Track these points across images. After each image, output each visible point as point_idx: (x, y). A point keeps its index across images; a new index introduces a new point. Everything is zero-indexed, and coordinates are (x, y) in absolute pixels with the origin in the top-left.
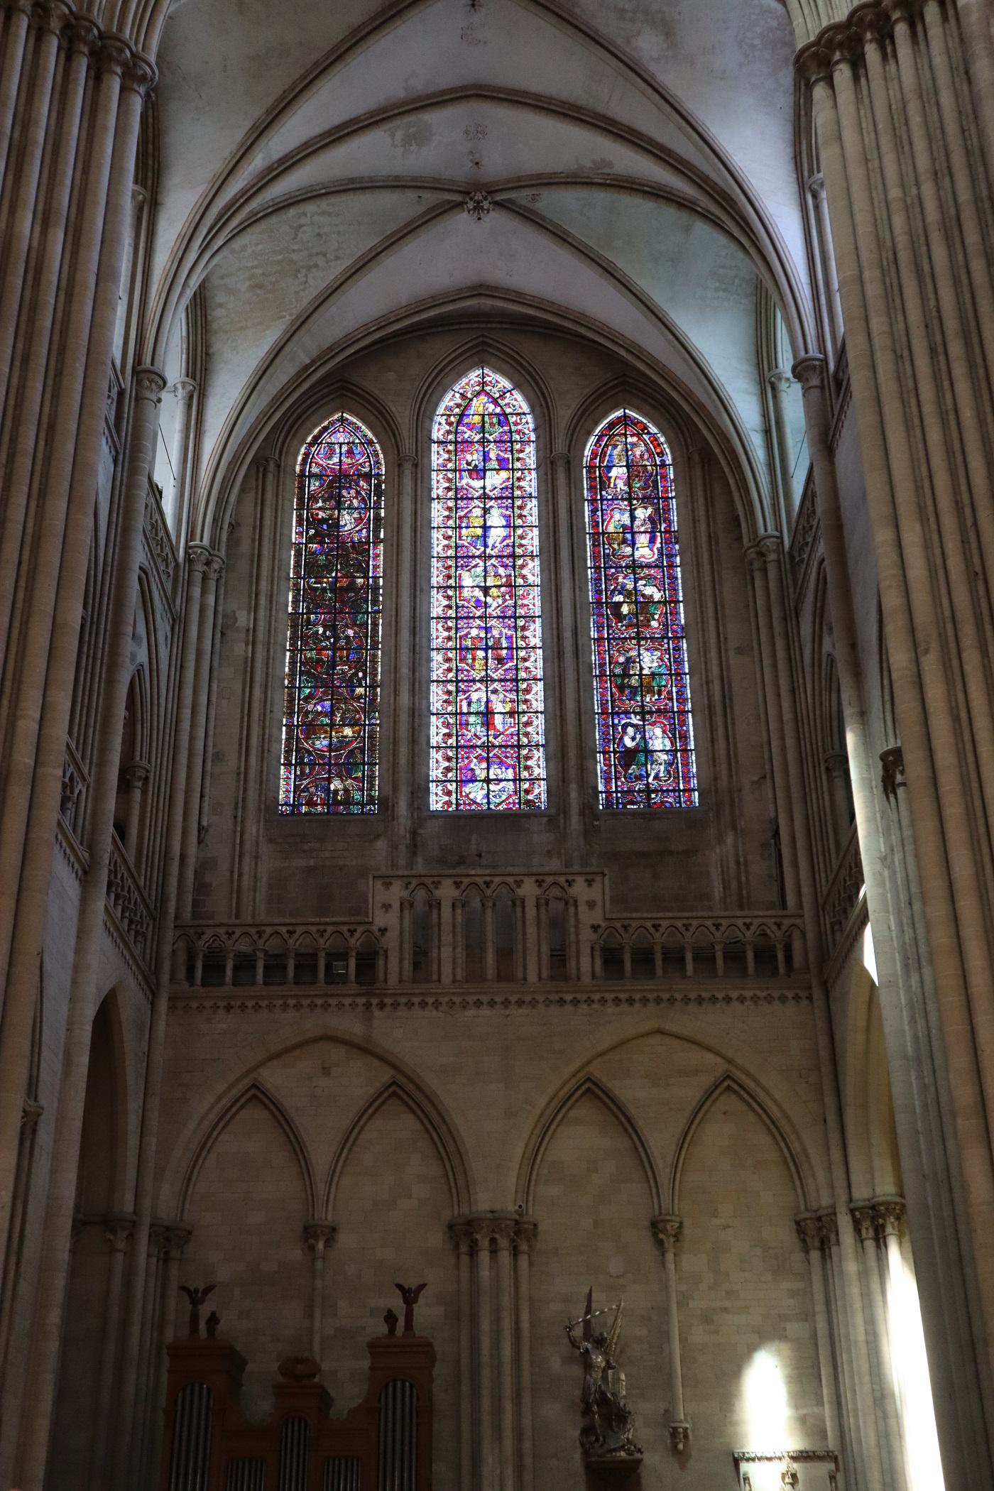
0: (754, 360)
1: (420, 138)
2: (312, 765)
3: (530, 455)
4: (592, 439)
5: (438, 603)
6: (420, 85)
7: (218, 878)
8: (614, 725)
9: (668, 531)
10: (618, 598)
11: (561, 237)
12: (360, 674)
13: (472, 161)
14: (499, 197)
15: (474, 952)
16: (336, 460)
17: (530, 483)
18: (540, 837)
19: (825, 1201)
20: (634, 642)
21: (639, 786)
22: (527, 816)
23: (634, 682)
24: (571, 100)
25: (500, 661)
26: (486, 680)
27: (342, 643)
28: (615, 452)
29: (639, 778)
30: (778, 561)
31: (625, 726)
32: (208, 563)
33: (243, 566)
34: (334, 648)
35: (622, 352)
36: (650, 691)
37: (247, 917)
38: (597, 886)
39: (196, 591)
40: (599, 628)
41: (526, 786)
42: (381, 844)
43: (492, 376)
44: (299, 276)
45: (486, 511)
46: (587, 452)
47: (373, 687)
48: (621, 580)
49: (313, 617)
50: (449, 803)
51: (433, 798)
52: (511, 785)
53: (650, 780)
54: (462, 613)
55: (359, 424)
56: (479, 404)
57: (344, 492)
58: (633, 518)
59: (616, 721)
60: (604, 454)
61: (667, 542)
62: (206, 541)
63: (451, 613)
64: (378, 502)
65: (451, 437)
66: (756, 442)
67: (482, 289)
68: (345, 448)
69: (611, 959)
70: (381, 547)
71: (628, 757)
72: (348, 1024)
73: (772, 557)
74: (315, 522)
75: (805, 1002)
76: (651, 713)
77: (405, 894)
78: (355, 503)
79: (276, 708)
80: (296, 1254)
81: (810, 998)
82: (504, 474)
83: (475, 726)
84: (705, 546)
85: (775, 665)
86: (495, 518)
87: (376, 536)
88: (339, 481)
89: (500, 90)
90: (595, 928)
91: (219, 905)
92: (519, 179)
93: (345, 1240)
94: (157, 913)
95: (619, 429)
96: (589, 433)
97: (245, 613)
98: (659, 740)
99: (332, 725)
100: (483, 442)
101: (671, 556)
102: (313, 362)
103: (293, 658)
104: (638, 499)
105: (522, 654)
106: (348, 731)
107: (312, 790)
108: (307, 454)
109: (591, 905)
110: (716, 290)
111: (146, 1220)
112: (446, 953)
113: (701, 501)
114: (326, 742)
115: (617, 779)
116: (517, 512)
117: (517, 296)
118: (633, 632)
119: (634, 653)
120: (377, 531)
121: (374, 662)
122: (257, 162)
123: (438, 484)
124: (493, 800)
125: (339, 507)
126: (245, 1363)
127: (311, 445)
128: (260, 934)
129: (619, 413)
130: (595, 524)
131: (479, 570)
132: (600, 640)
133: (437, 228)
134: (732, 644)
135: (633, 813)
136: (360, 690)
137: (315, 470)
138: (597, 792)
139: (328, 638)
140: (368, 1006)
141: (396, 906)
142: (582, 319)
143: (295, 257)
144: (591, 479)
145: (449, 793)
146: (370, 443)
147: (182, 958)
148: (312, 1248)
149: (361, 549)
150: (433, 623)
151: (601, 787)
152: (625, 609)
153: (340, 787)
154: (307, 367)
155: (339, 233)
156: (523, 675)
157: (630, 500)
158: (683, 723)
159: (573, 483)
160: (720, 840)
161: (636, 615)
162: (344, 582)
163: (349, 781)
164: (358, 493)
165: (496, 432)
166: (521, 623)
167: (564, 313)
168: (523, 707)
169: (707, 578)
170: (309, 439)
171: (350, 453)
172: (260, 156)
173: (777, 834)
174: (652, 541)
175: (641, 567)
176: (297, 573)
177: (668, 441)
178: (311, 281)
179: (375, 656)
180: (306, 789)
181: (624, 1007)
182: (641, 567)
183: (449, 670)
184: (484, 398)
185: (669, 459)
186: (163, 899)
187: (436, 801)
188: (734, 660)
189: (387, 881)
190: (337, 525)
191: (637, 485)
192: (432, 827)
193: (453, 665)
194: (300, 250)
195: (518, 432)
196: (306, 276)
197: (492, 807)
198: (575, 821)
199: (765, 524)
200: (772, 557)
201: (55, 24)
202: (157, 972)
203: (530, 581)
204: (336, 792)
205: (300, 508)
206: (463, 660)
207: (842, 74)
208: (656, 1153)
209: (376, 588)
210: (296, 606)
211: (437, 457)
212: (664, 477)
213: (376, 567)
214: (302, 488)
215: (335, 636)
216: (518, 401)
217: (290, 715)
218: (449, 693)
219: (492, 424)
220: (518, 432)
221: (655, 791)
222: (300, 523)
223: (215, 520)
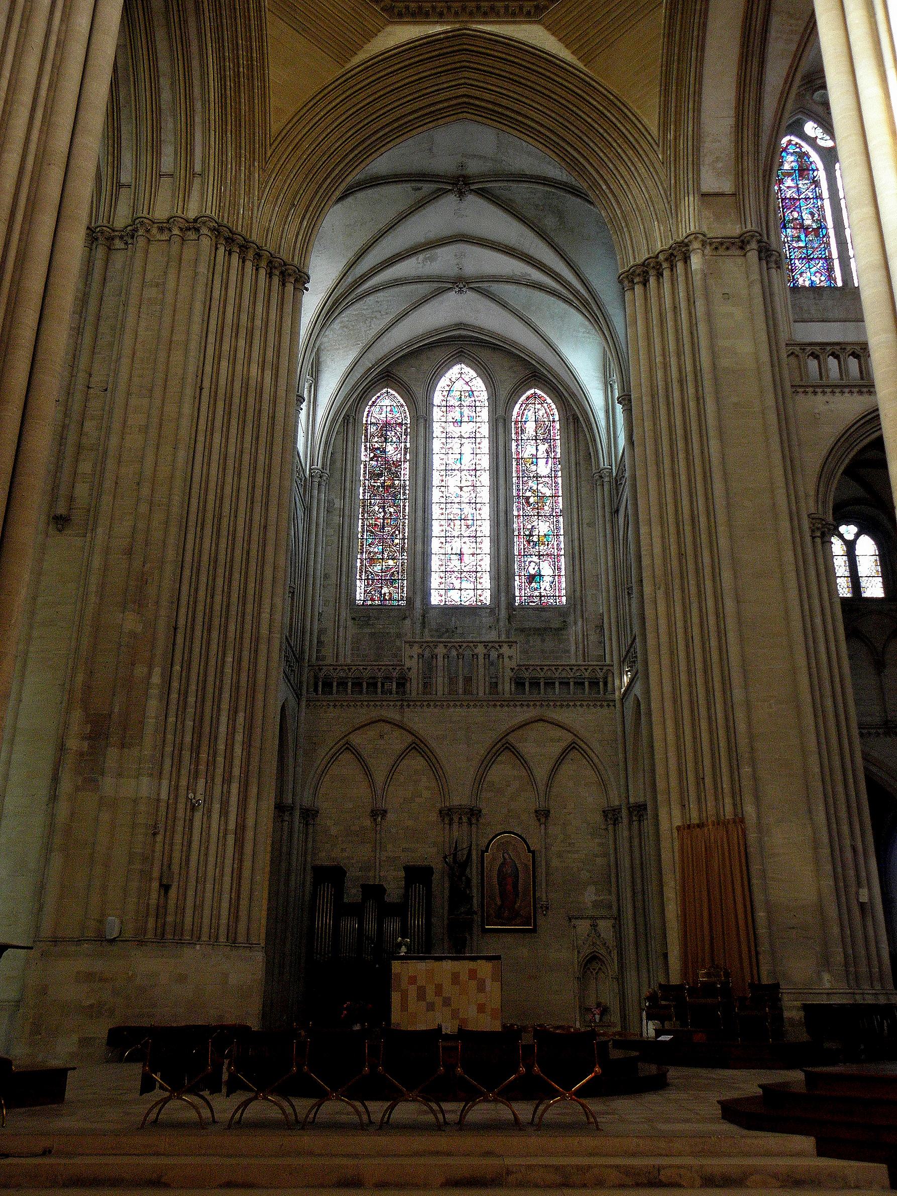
1: (432, 259)
2: (373, 580)
3: (484, 414)
4: (518, 406)
5: (436, 495)
6: (432, 236)
7: (327, 639)
10: (528, 494)
11: (504, 305)
14: (472, 286)
15: (452, 681)
16: (384, 415)
17: (485, 430)
18: (487, 620)
19: (617, 803)
21: (536, 593)
22: (480, 608)
23: (535, 539)
24: (511, 245)
25: (468, 526)
26: (460, 536)
27: (388, 516)
29: (536, 589)
31: (530, 562)
33: (337, 475)
34: (384, 519)
35: (534, 362)
37: (341, 660)
38: (514, 647)
40: (519, 510)
41: (479, 592)
42: (408, 622)
43: (466, 369)
46: (515, 413)
47: (403, 539)
52: (471, 593)
53: (542, 590)
55: (396, 395)
56: (459, 385)
57: (389, 433)
58: (537, 450)
60: (523, 414)
62: (320, 466)
63: (443, 500)
64: (406, 439)
65: (444, 403)
66: (602, 423)
67: (460, 326)
68: (389, 408)
69: (519, 683)
71: (531, 578)
72: (393, 714)
73: (607, 479)
74: (373, 450)
77: (420, 651)
78: (394, 439)
80: (368, 823)
81: (614, 706)
83: (455, 562)
84: (573, 467)
86: (467, 448)
87: (405, 458)
88: (386, 426)
89: (474, 238)
90: (512, 669)
91: (328, 651)
92: (482, 277)
93: (390, 816)
94: (299, 660)
95: (531, 401)
98: (546, 569)
99: (382, 559)
100: (461, 406)
102: (373, 366)
106: (391, 562)
108: (369, 411)
109: (510, 657)
111: (298, 807)
112: (440, 680)
113: (573, 442)
114: (380, 568)
116: (478, 446)
117: (480, 330)
119: (535, 523)
120: (405, 454)
122: (350, 279)
123: (437, 429)
125: (386, 441)
126: (345, 873)
127: (371, 406)
128: (349, 669)
129: (532, 391)
130: (518, 453)
132: (519, 516)
133: (440, 299)
134: (585, 521)
135: (533, 608)
137: (373, 420)
138: (515, 597)
140: (402, 706)
141: (416, 656)
142: (514, 344)
144: (517, 428)
145: (441, 596)
146: (402, 406)
147: (312, 682)
148: (375, 820)
149: (397, 464)
151: (517, 594)
152: (532, 500)
154: (371, 368)
157: (536, 440)
158: (559, 561)
159: (507, 431)
162: (388, 483)
165: (468, 401)
166: (478, 506)
167: (505, 340)
168: (479, 551)
169: (574, 486)
170: (370, 403)
171: (391, 411)
176: (364, 477)
181: (525, 708)
184: (461, 382)
185: (557, 418)
186: (302, 652)
187: (435, 600)
188: (586, 530)
189: (411, 644)
190: (384, 451)
192: (432, 614)
198: (503, 613)
199: (604, 463)
200: (607, 479)
201: (263, 264)
202: (300, 689)
207: (638, 289)
208: (538, 779)
209: (405, 486)
211: (437, 414)
214: (366, 430)
215: (384, 511)
216: (479, 384)
217: (362, 553)
222: (366, 451)
223: (324, 453)
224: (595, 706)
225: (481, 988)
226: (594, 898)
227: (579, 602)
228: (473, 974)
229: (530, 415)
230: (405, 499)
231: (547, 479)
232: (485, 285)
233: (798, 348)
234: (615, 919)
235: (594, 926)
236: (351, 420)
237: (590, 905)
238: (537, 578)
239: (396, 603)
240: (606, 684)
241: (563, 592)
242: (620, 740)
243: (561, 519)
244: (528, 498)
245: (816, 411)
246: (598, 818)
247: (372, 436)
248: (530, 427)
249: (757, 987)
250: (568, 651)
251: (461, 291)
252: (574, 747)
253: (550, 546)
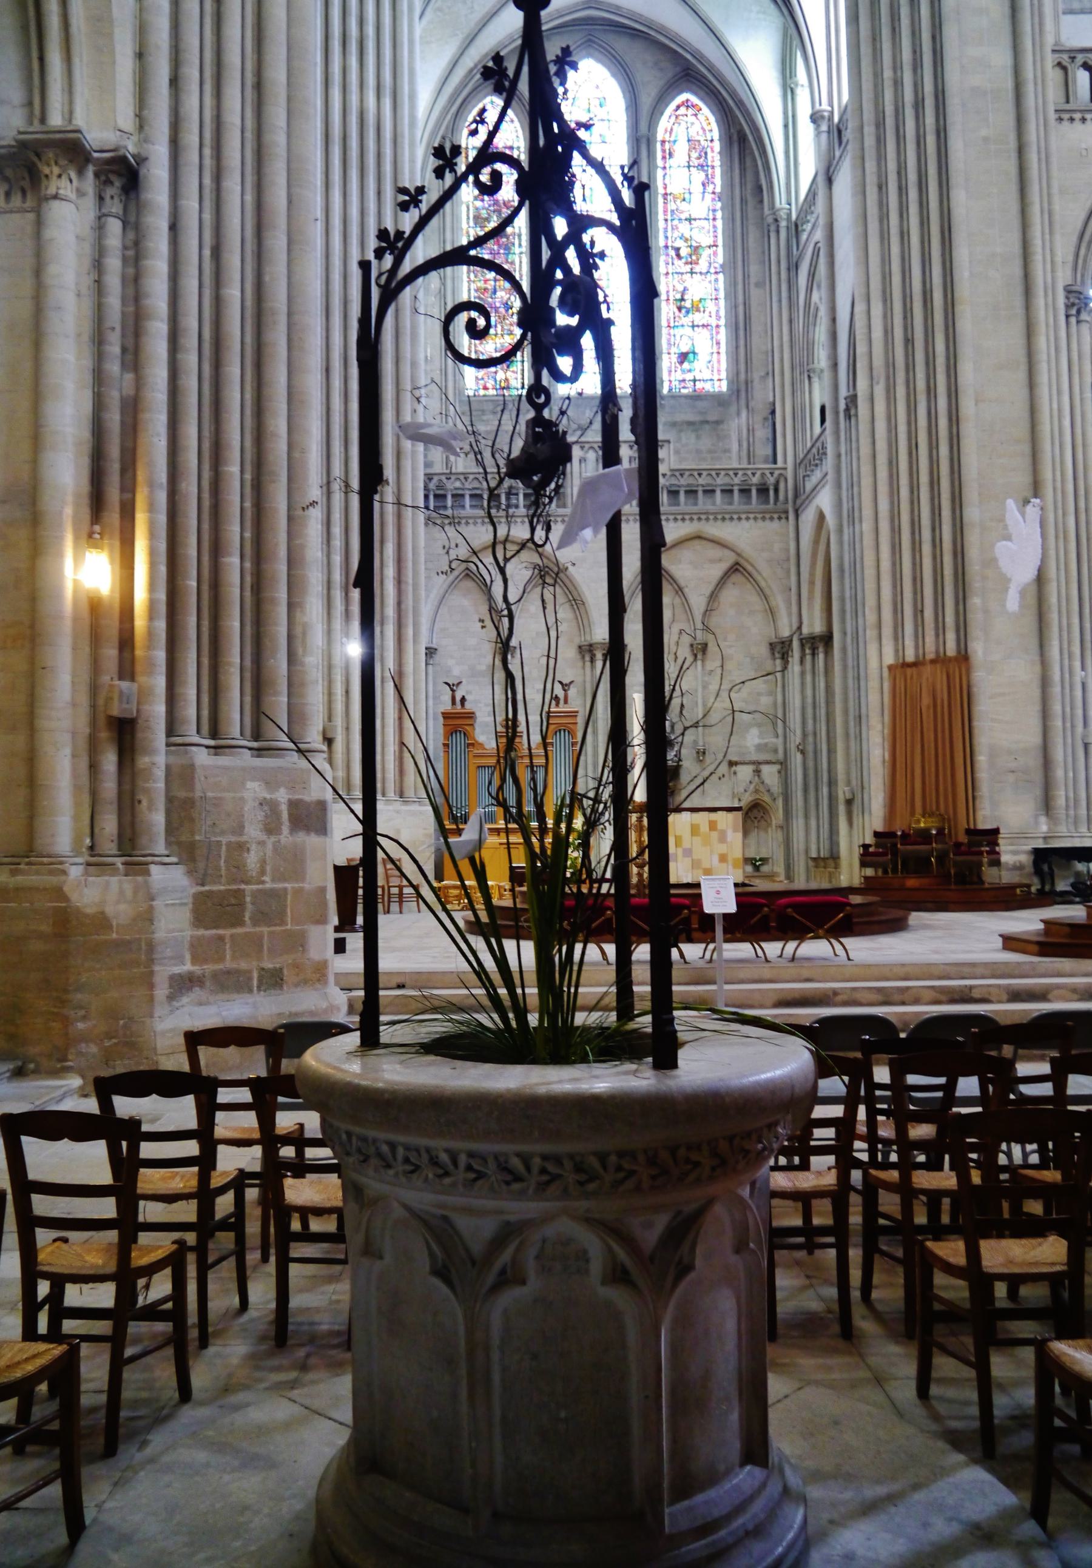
0: (779, 66)
9: (714, 193)
10: (677, 244)
19: (785, 633)
29: (690, 371)
30: (788, 228)
35: (689, 57)
36: (698, 310)
61: (714, 199)
71: (683, 357)
75: (783, 521)
81: (787, 518)
95: (683, 110)
101: (714, 211)
110: (758, 12)
113: (737, 172)
114: (494, 346)
118: (688, 268)
128: (466, 479)
132: (667, 274)
134: (753, 280)
135: (686, 397)
142: (661, 30)
144: (664, 151)
157: (689, 167)
159: (651, 155)
160: (738, 414)
173: (773, 412)
175: (695, 220)
181: (680, 523)
182: (695, 220)
188: (755, 293)
191: (694, 155)
199: (780, 201)
200: (783, 224)
209: (520, 236)
224: (764, 519)
225: (722, 839)
226: (757, 741)
227: (743, 388)
228: (713, 826)
229: (680, 133)
230: (521, 253)
231: (705, 223)
233: (1065, 56)
234: (781, 764)
235: (757, 772)
237: (752, 749)
238: (691, 356)
240: (776, 490)
241: (724, 375)
242: (793, 560)
243: (721, 277)
244: (677, 250)
245: (1084, 146)
246: (764, 650)
248: (681, 150)
249: (973, 832)
250: (727, 451)
252: (737, 570)
253: (707, 313)
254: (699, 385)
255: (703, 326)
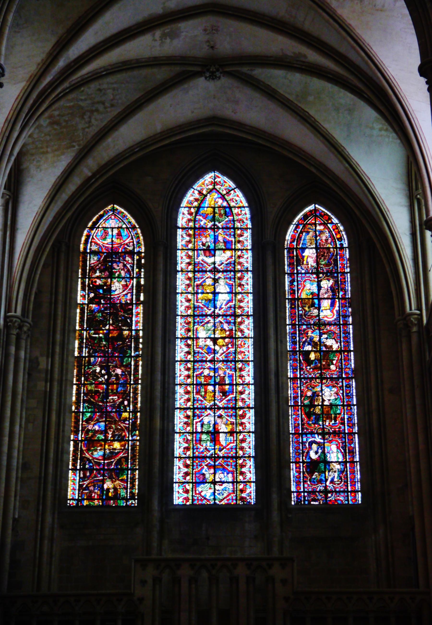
1: (174, 35)
4: (292, 227)
8: (303, 443)
9: (344, 298)
10: (308, 348)
12: (126, 403)
13: (208, 46)
14: (227, 69)
16: (109, 240)
20: (318, 380)
21: (320, 487)
25: (224, 393)
26: (214, 408)
27: (113, 379)
28: (308, 237)
29: (320, 481)
31: (311, 443)
32: (20, 327)
34: (108, 383)
36: (329, 417)
39: (13, 349)
40: (294, 369)
41: (241, 486)
43: (222, 178)
44: (85, 117)
45: (216, 281)
46: (288, 237)
48: (310, 334)
49: (92, 359)
50: (187, 499)
51: (176, 495)
52: (230, 486)
53: (328, 483)
54: (198, 358)
55: (126, 213)
57: (115, 265)
58: (319, 287)
59: (305, 439)
60: (300, 238)
61: (343, 306)
63: (190, 357)
64: (139, 273)
65: (191, 224)
68: (115, 231)
70: (141, 308)
73: (415, 329)
74: (94, 288)
76: (329, 434)
78: (123, 273)
79: (67, 428)
82: (228, 253)
85: (414, 408)
86: (222, 287)
87: (138, 299)
96: (290, 223)
97: (45, 358)
99: (106, 440)
100: (214, 228)
101: (345, 316)
102: (94, 175)
103: (78, 390)
104: (323, 273)
105: (240, 388)
106: (117, 445)
107: (92, 488)
108: (88, 236)
109: (284, 582)
110: (380, 130)
114: (101, 453)
115: (305, 482)
118: (317, 373)
119: (318, 389)
121: (135, 393)
124: (217, 496)
127: (92, 228)
130: (293, 292)
131: (210, 325)
132: (294, 379)
136: (125, 415)
137: (94, 248)
138: (291, 492)
139: (103, 376)
143: (82, 104)
144: (291, 258)
145: (187, 492)
146: (134, 228)
150: (177, 365)
151: (293, 488)
152: (312, 356)
153: (111, 486)
155: (114, 89)
156: (240, 404)
157: (317, 273)
158: (351, 441)
161: (320, 361)
162: (115, 334)
163: (117, 482)
164: (125, 266)
166: (239, 365)
170: (90, 224)
171: (119, 235)
172: (63, 59)
174: (333, 305)
176: (81, 325)
177: (345, 230)
178: (93, 121)
179: (136, 389)
180: (87, 488)
182: (325, 324)
183: (188, 400)
184: (215, 195)
185: (346, 245)
190: (109, 290)
193: (191, 396)
194: (85, 100)
195: (239, 221)
196: (90, 117)
197: (217, 502)
198: (275, 516)
203: (246, 334)
204: (108, 490)
205: (83, 277)
206: (198, 393)
209: (137, 337)
210: (80, 351)
212: (342, 257)
213: (137, 322)
215: (110, 376)
217: (76, 433)
218: (188, 417)
219: (221, 215)
220: (239, 221)
221: (331, 492)
222: (83, 289)
223: (25, 295)
230: (137, 356)
232: (245, 69)
236: (64, 248)
239: (122, 503)
247: (93, 269)
251: (213, 77)
254: (331, 497)
255: (335, 433)
